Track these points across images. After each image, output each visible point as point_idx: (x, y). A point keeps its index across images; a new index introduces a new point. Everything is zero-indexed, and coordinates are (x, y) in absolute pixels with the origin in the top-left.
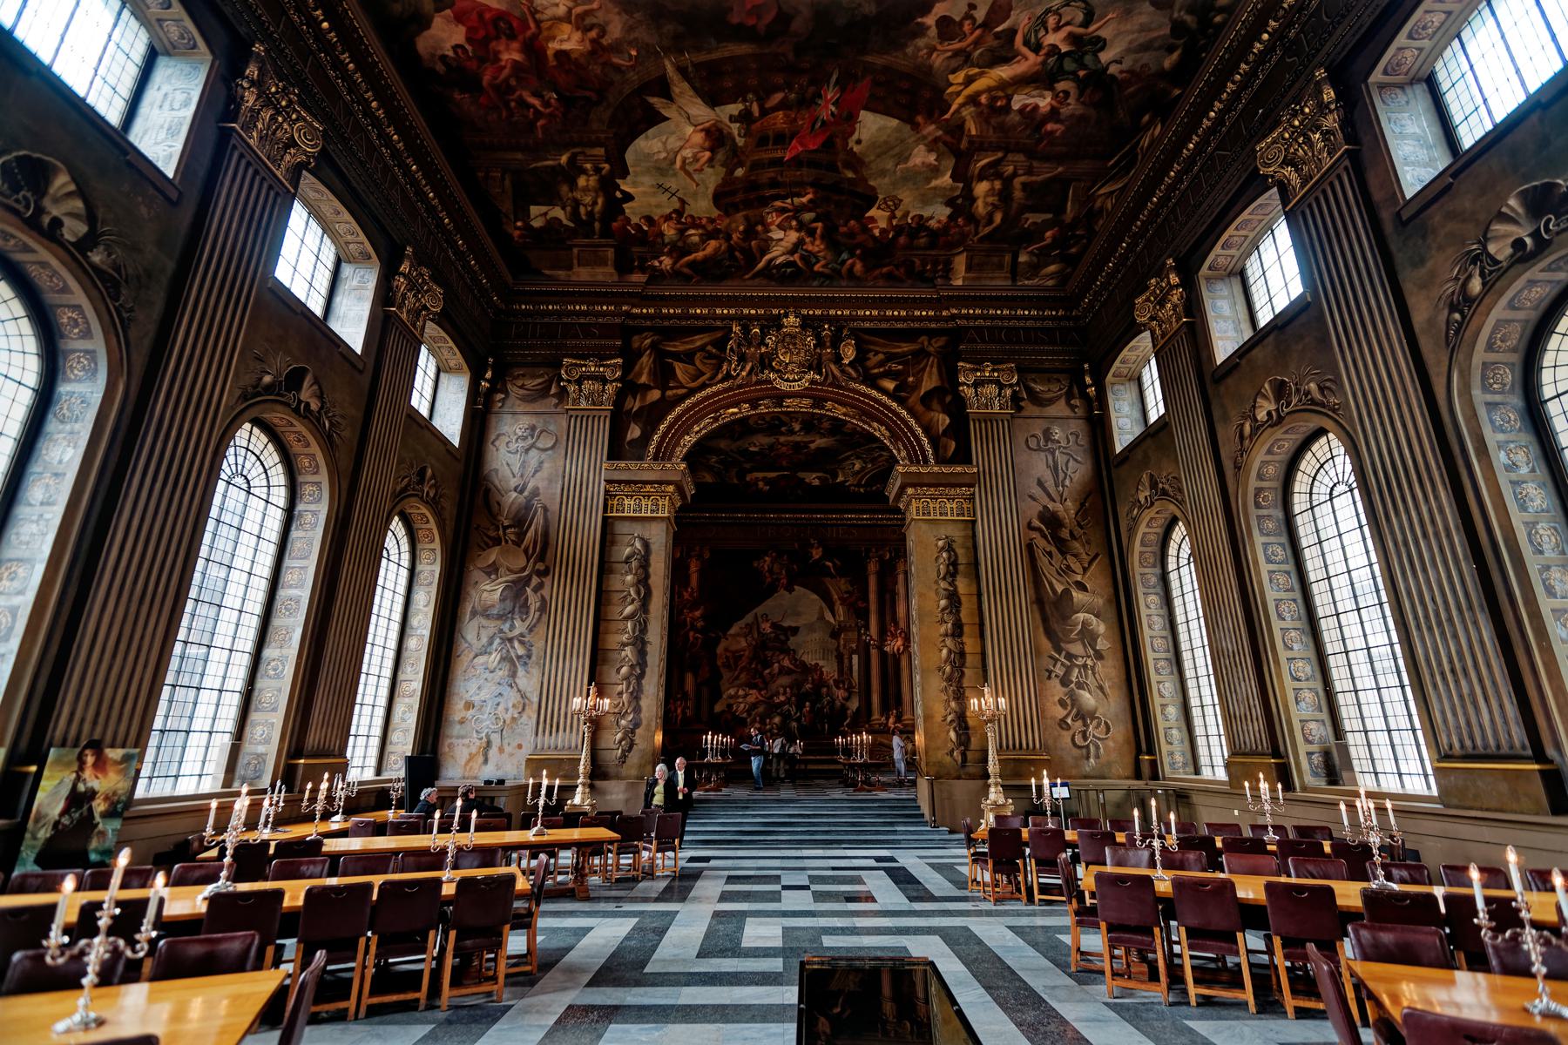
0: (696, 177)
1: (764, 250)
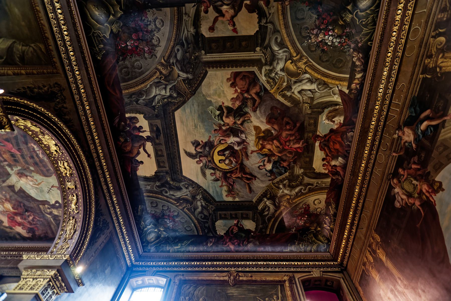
0: (40, 182)
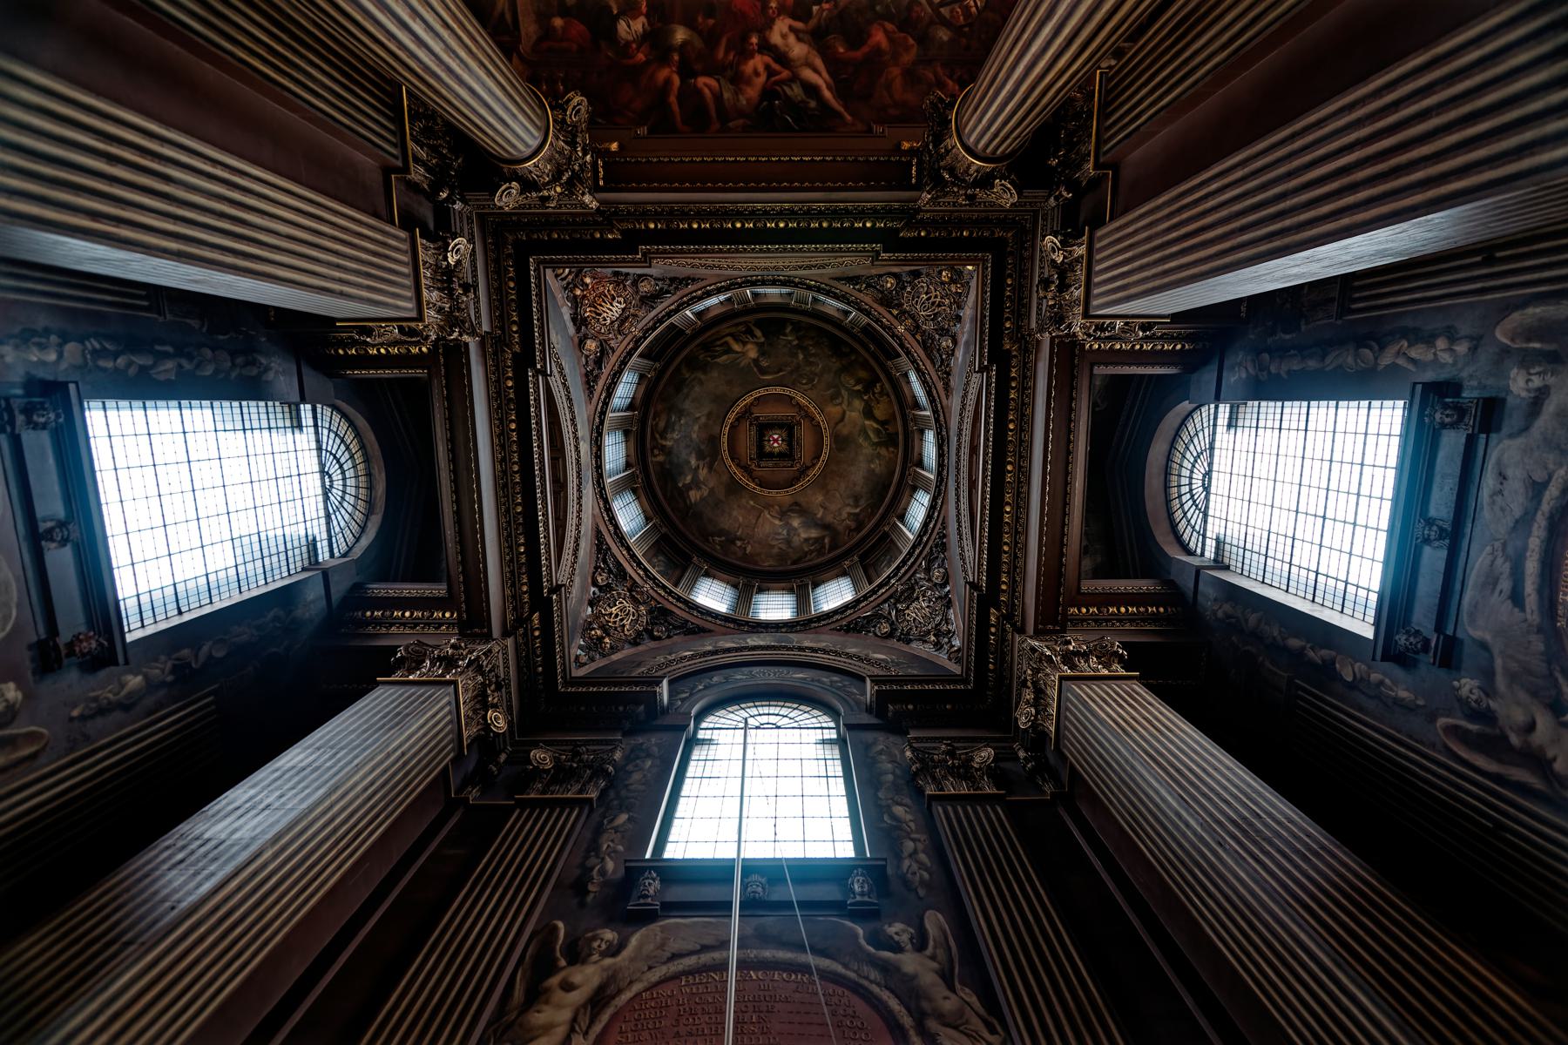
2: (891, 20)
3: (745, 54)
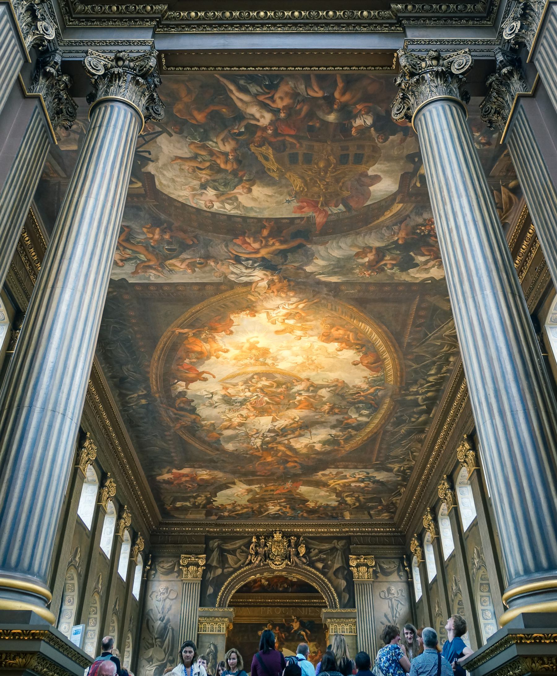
1: (266, 511)
2: (193, 125)
3: (289, 109)
